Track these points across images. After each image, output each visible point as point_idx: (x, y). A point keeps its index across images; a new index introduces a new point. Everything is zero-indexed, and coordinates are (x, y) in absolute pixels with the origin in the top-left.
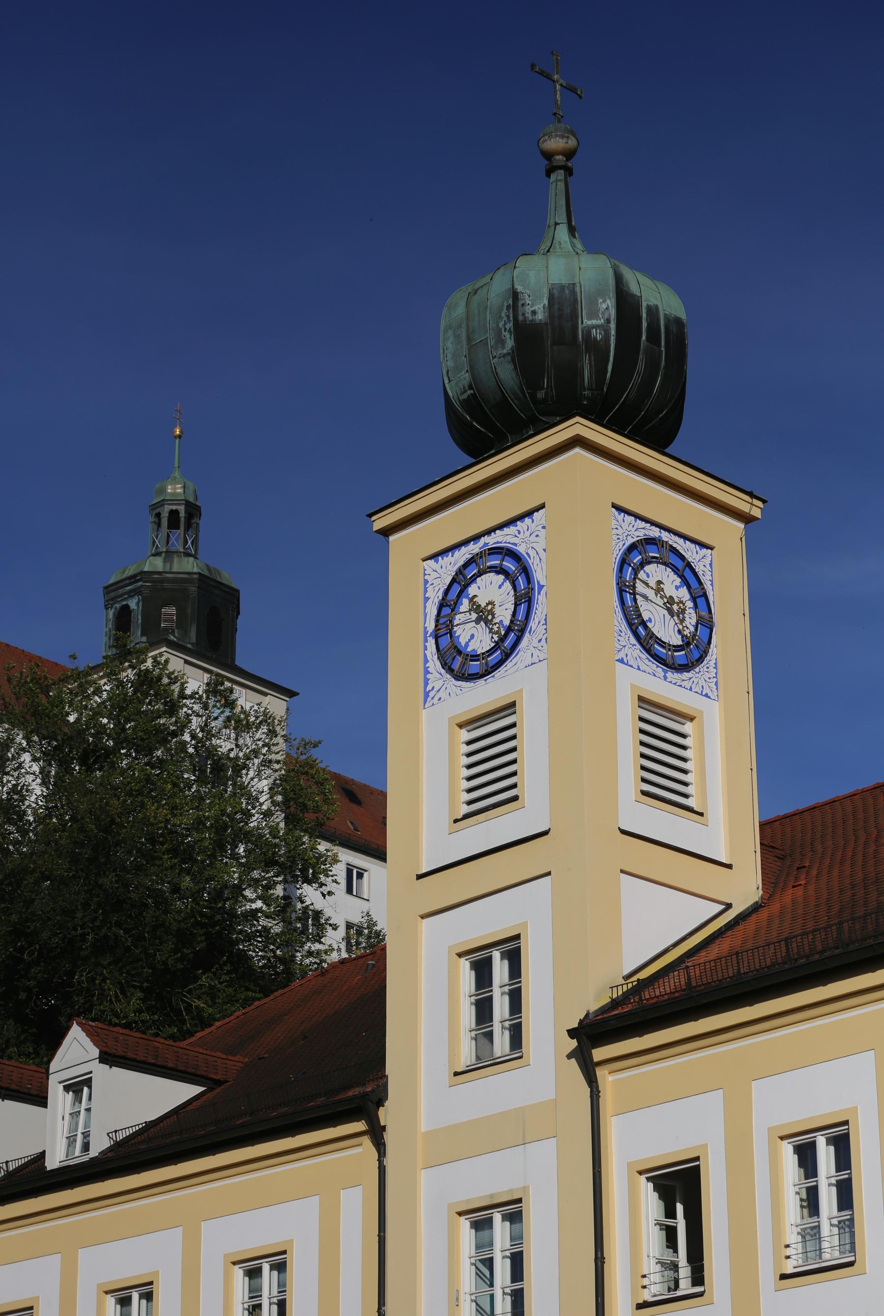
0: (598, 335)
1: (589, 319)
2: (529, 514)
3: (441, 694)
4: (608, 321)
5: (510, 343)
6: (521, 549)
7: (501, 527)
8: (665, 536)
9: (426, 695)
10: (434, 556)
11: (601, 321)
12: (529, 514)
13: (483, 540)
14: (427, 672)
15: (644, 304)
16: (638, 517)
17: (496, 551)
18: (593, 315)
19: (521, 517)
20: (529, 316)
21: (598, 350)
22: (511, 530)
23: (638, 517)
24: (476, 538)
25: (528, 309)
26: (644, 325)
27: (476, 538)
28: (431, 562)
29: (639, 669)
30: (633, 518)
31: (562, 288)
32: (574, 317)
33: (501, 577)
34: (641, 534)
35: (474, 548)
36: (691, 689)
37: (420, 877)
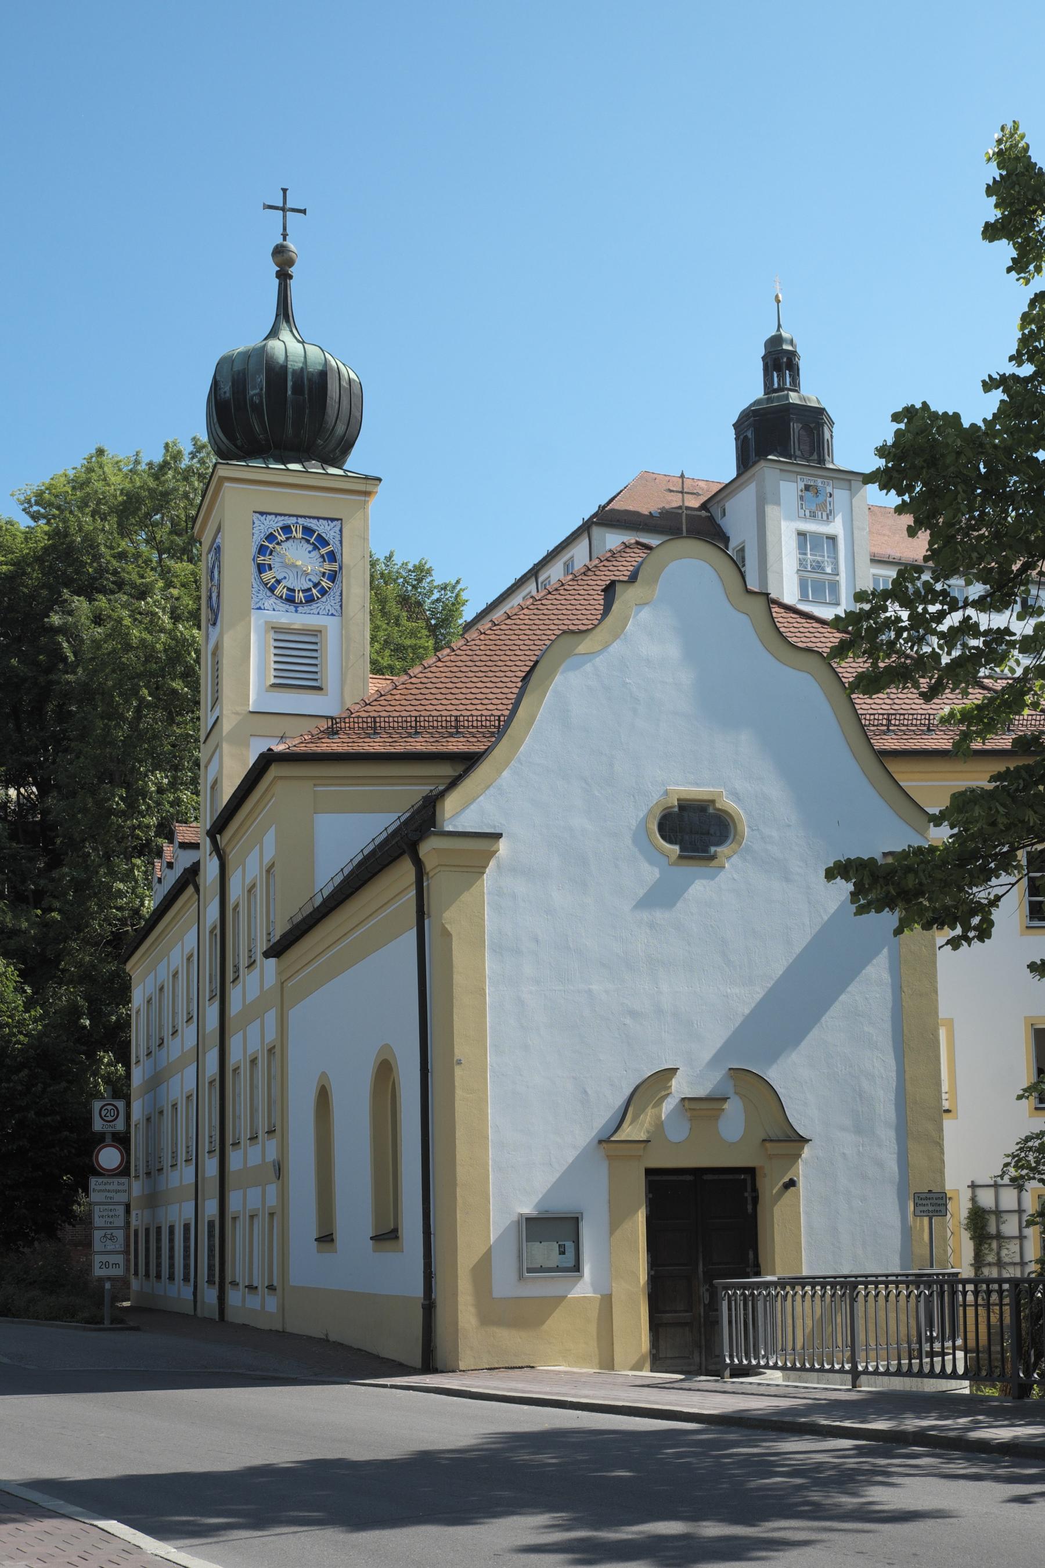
0: (256, 400)
1: (252, 390)
4: (261, 389)
8: (301, 521)
11: (257, 391)
15: (290, 371)
16: (276, 515)
18: (254, 388)
20: (223, 396)
21: (257, 408)
23: (276, 515)
25: (222, 391)
26: (290, 384)
29: (274, 610)
30: (273, 516)
31: (239, 372)
32: (244, 391)
34: (281, 524)
36: (318, 614)
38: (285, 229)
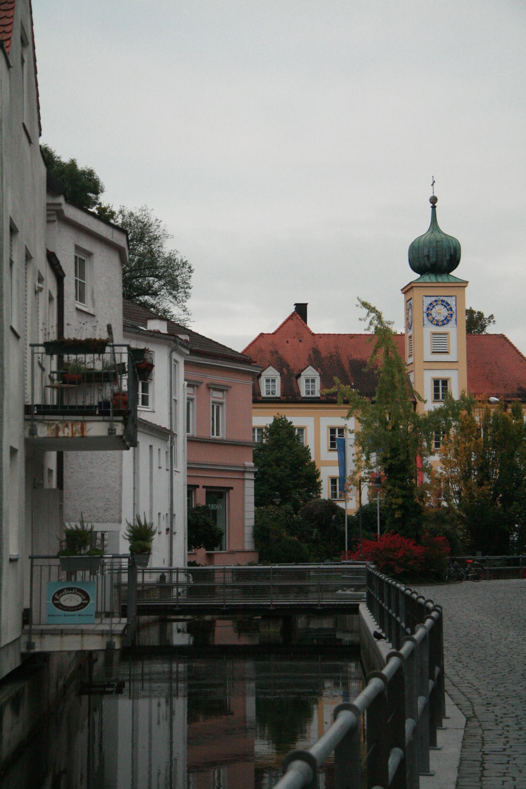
2: (451, 296)
3: (428, 326)
5: (448, 258)
6: (449, 303)
7: (444, 296)
9: (424, 325)
10: (426, 296)
12: (451, 296)
13: (438, 297)
14: (424, 320)
17: (443, 301)
19: (449, 296)
22: (446, 298)
24: (437, 296)
27: (437, 296)
28: (425, 297)
33: (443, 307)
35: (437, 298)
37: (424, 362)
38: (434, 207)
